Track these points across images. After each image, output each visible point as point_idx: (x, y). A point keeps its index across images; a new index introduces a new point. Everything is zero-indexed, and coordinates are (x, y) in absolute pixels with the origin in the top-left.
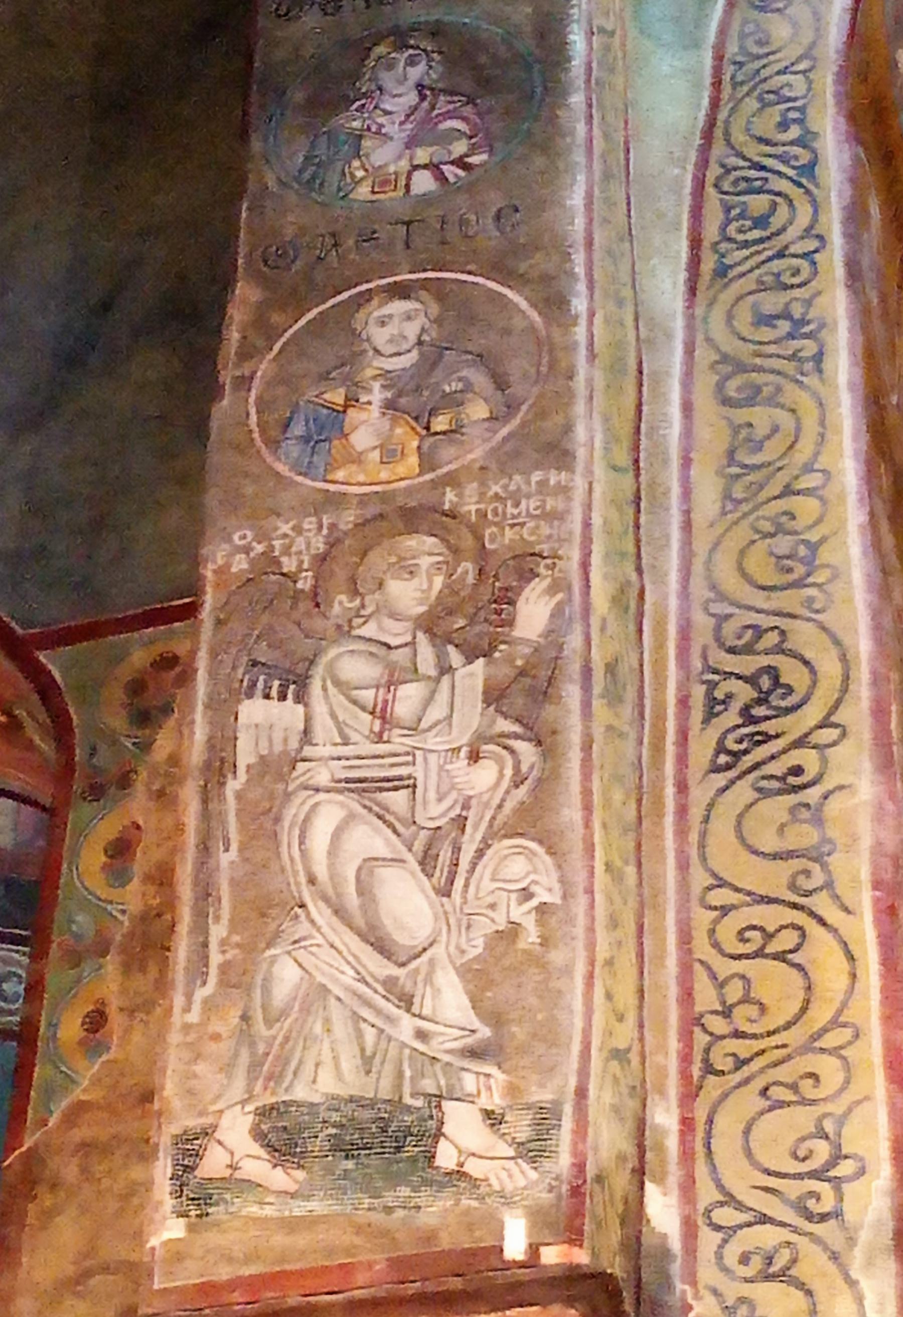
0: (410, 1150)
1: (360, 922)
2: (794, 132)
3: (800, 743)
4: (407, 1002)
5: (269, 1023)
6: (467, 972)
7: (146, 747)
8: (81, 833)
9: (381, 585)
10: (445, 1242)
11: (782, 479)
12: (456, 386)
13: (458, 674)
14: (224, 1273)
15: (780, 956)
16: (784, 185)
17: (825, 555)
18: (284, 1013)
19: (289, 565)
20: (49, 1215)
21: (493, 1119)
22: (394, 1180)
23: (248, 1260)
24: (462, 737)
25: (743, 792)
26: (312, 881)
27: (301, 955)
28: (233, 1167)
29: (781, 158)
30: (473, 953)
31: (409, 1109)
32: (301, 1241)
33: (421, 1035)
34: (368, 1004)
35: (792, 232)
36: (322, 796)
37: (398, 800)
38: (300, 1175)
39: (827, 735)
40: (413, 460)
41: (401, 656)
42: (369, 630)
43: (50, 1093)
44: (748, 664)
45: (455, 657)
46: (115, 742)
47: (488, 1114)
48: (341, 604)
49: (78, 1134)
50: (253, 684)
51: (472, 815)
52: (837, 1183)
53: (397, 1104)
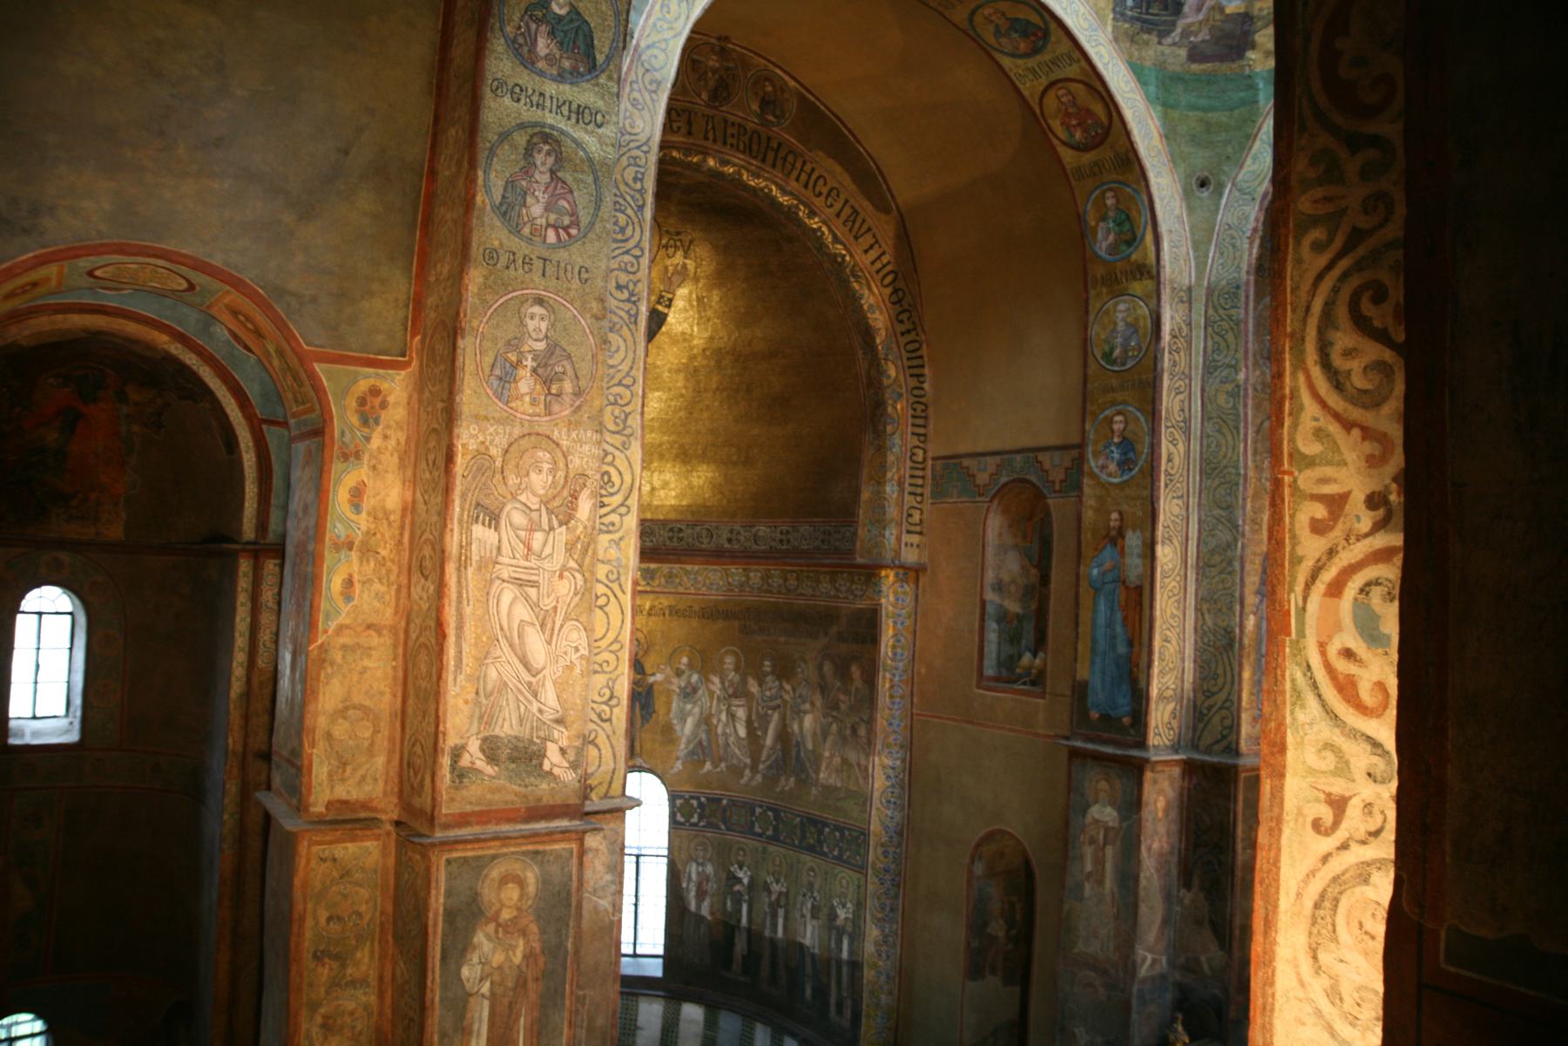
0: (534, 762)
1: (520, 653)
2: (638, 186)
3: (613, 511)
4: (535, 695)
5: (487, 697)
6: (555, 682)
7: (368, 439)
8: (339, 481)
9: (528, 474)
10: (545, 800)
11: (619, 376)
12: (561, 369)
13: (557, 531)
14: (469, 808)
15: (601, 608)
16: (629, 211)
17: (629, 422)
18: (491, 695)
19: (493, 451)
20: (329, 677)
21: (563, 751)
22: (529, 774)
23: (478, 804)
26: (502, 629)
27: (498, 665)
28: (473, 763)
29: (632, 197)
30: (558, 674)
31: (535, 744)
32: (497, 797)
33: (540, 711)
34: (522, 693)
35: (632, 243)
36: (505, 585)
37: (532, 592)
38: (496, 768)
39: (623, 510)
40: (542, 406)
41: (535, 515)
42: (523, 498)
43: (328, 616)
45: (555, 523)
46: (352, 431)
47: (561, 749)
48: (512, 480)
49: (342, 640)
50: (478, 517)
51: (559, 606)
52: (611, 707)
53: (531, 741)
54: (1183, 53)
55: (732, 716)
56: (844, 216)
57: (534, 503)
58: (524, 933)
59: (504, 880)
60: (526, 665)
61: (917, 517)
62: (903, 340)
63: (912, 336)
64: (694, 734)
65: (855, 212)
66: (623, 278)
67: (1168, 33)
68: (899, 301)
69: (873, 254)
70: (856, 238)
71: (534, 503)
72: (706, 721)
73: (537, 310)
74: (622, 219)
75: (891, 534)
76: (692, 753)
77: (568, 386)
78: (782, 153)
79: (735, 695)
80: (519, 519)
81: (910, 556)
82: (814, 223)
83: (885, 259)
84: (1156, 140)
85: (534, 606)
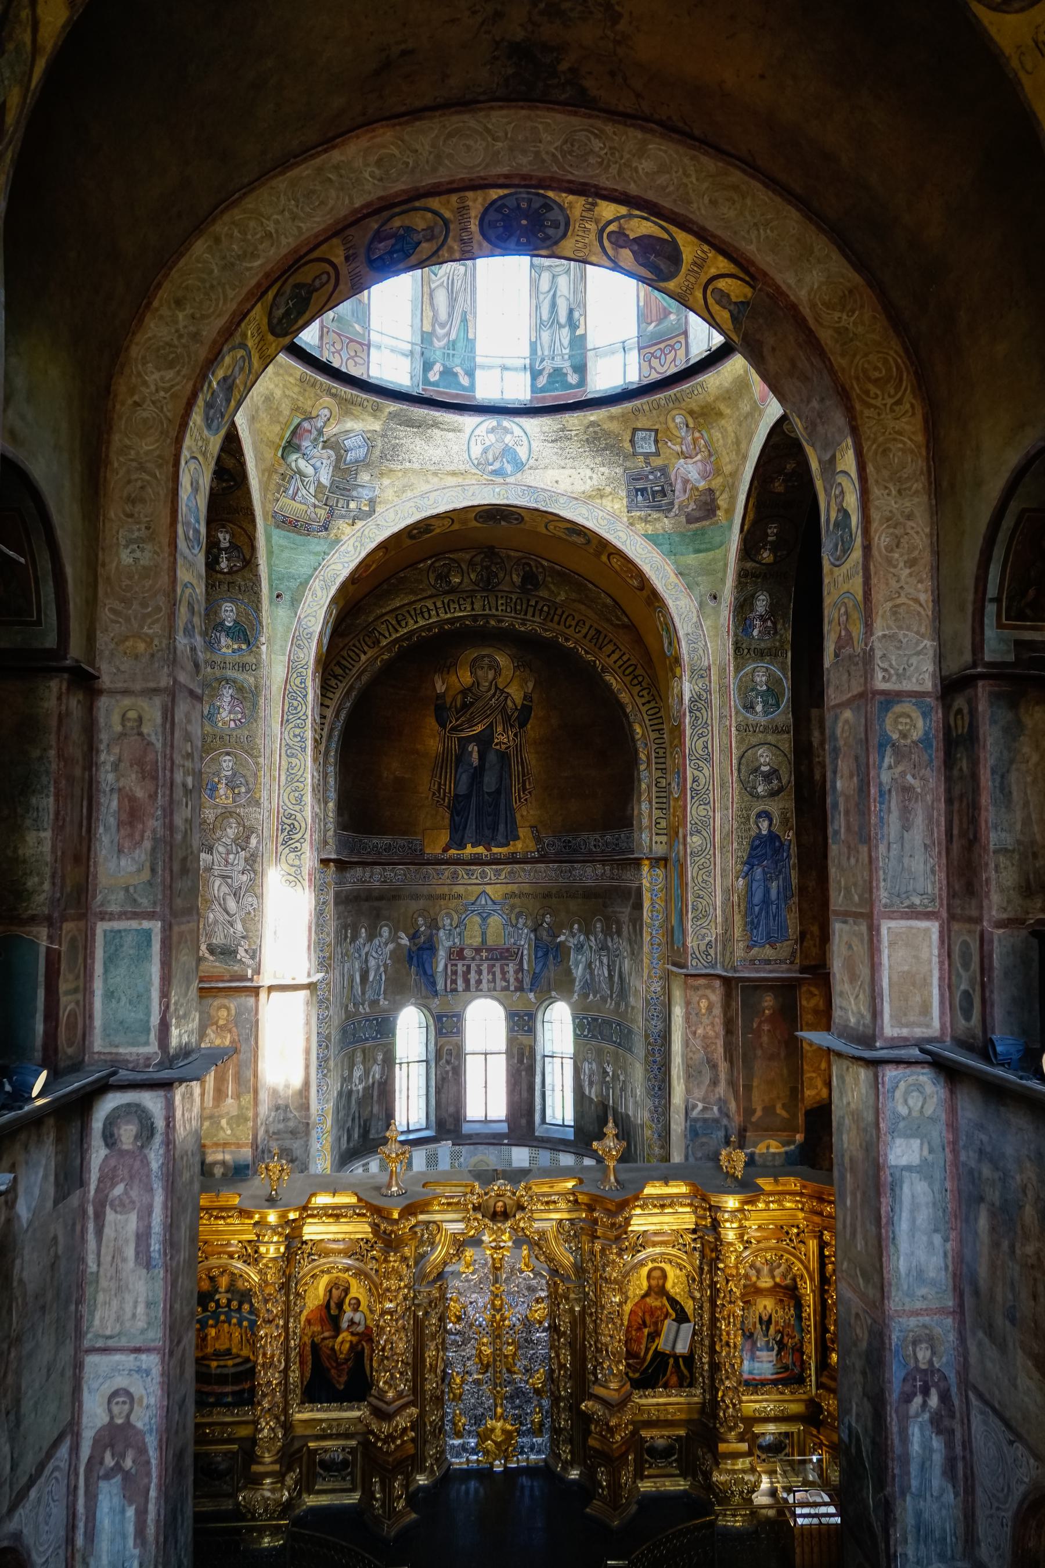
24: (240, 868)
25: (287, 850)
44: (289, 822)
48: (219, 833)
54: (683, 519)
55: (601, 962)
56: (589, 637)
57: (229, 841)
58: (230, 1031)
59: (219, 1008)
60: (228, 913)
61: (663, 824)
62: (644, 709)
63: (653, 704)
64: (583, 975)
65: (598, 632)
66: (297, 731)
67: (670, 510)
68: (640, 683)
69: (615, 656)
70: (600, 649)
71: (229, 841)
72: (589, 966)
73: (228, 758)
74: (295, 703)
75: (645, 836)
76: (583, 988)
77: (243, 790)
78: (539, 607)
79: (602, 949)
80: (221, 849)
81: (659, 850)
82: (570, 644)
83: (625, 658)
84: (673, 578)
85: (230, 886)
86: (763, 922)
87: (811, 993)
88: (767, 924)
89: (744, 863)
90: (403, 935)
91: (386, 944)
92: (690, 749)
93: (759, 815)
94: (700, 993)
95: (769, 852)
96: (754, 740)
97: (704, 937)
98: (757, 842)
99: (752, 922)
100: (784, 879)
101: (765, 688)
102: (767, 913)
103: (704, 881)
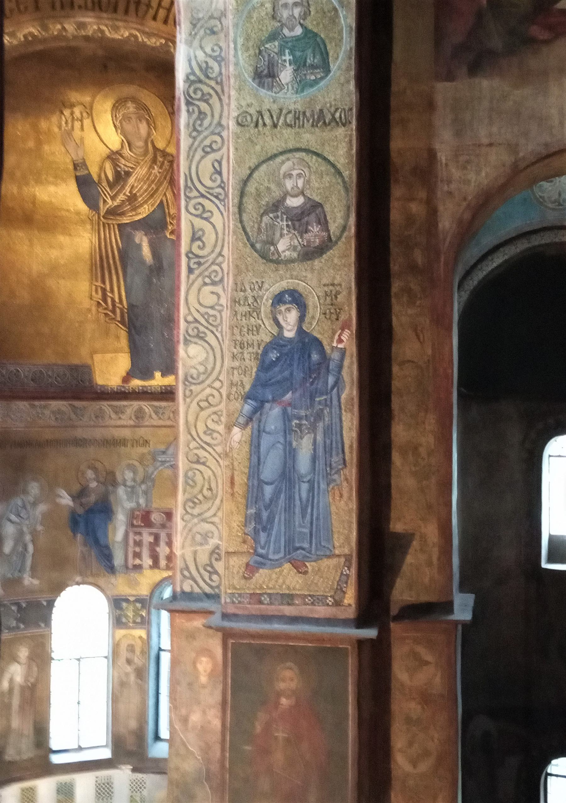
86: (280, 518)
87: (416, 656)
88: (289, 523)
89: (247, 397)
90: (63, 493)
91: (34, 504)
92: (189, 177)
93: (279, 299)
94: (197, 644)
95: (298, 375)
96: (275, 145)
97: (206, 536)
98: (273, 355)
99: (258, 517)
100: (328, 431)
101: (298, 31)
102: (290, 499)
103: (209, 431)
